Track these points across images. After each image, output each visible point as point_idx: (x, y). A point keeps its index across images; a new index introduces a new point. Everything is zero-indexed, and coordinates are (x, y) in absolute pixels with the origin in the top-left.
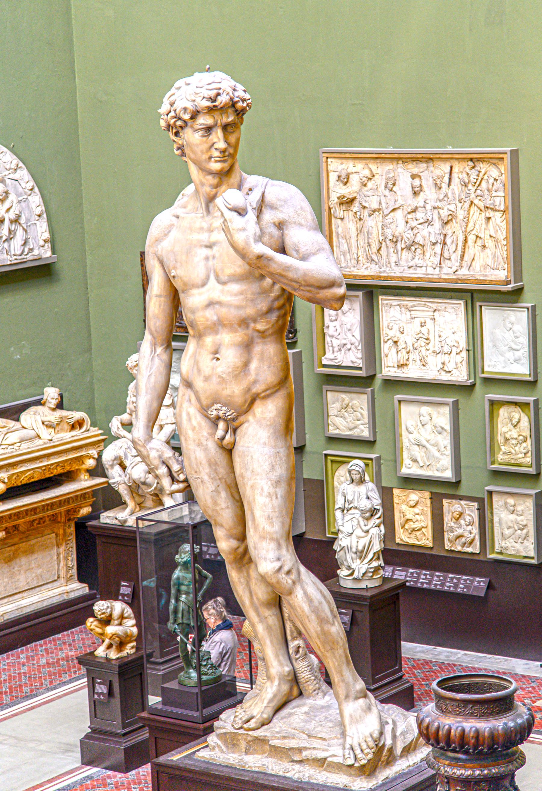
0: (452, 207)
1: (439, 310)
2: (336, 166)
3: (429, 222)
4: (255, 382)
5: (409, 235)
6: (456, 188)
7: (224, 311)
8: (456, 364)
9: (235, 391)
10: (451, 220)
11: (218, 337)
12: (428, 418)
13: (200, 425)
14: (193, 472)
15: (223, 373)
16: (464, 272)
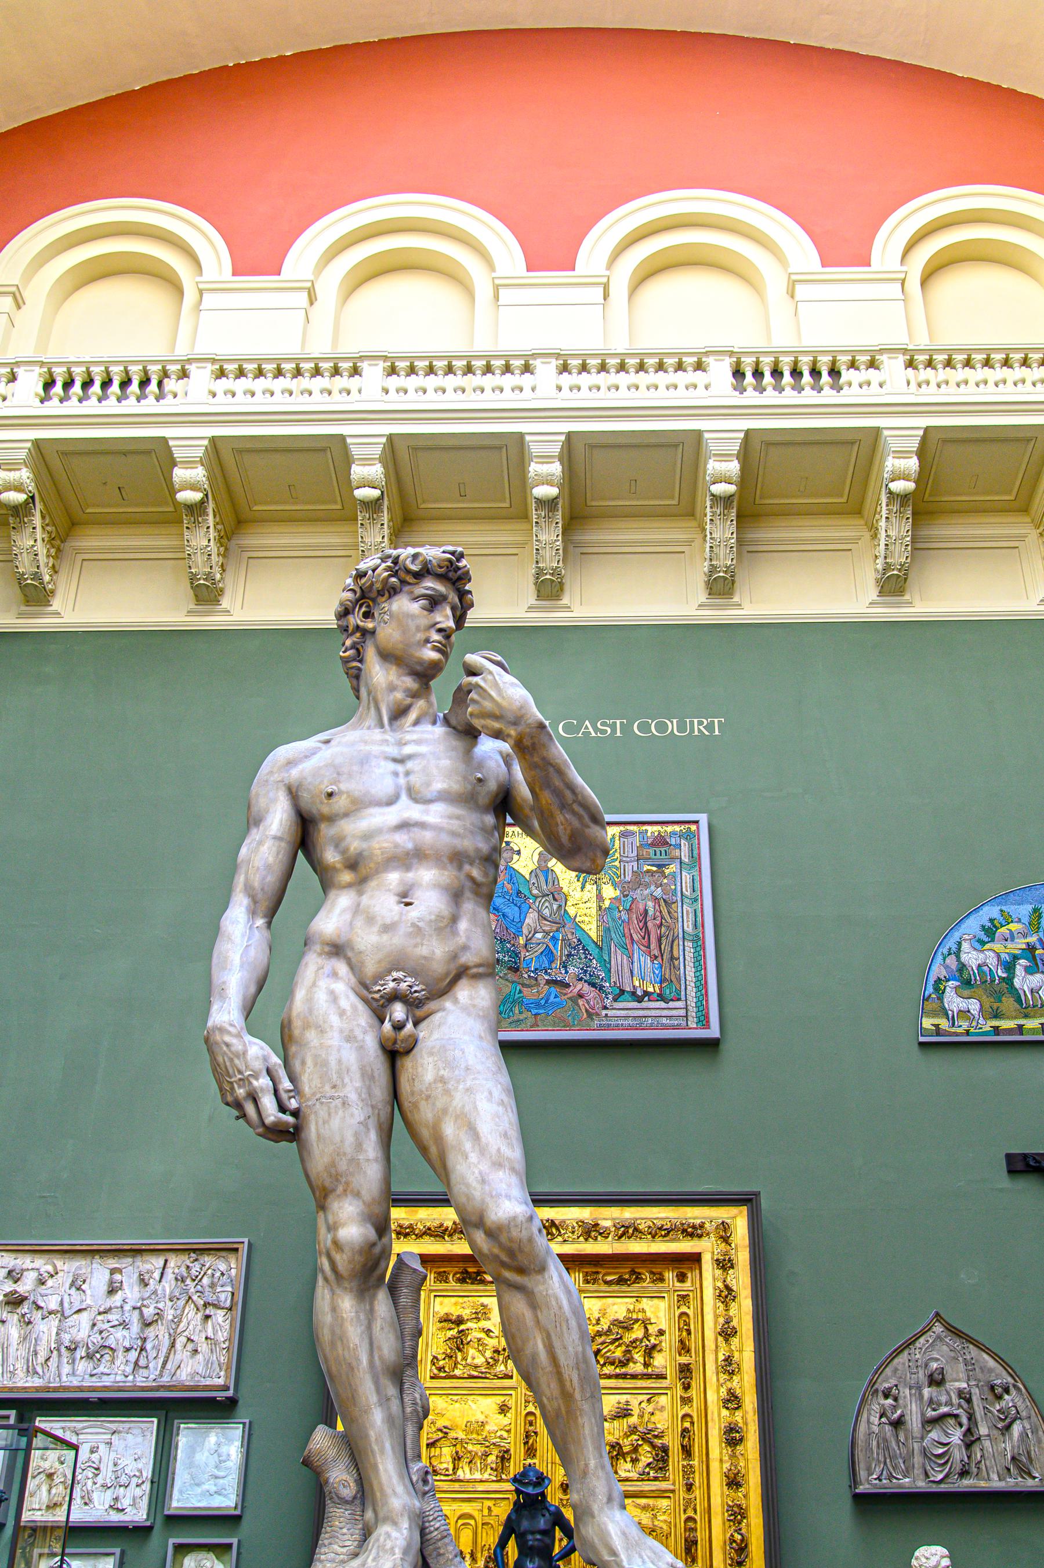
0: (161, 1305)
1: (120, 1432)
3: (124, 1325)
4: (465, 948)
5: (96, 1338)
6: (167, 1286)
7: (428, 836)
9: (435, 951)
10: (157, 1321)
11: (410, 875)
13: (354, 1008)
14: (327, 1088)
15: (420, 919)
16: (166, 1379)
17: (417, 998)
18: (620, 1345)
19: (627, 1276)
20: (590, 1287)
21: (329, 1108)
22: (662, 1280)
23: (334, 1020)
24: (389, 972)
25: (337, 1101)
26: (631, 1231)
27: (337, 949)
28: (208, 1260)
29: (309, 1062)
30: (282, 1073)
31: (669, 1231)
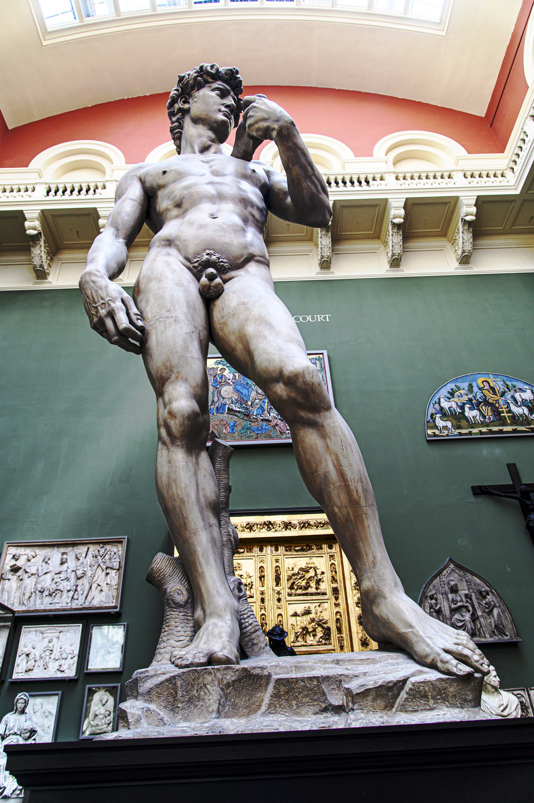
0: (85, 569)
1: (64, 632)
2: (13, 551)
3: (67, 579)
5: (54, 586)
8: (69, 665)
10: (83, 577)
12: (40, 706)
14: (164, 312)
16: (87, 605)
17: (223, 266)
18: (304, 580)
19: (305, 548)
20: (288, 553)
21: (165, 324)
22: (321, 548)
23: (169, 274)
24: (204, 250)
25: (170, 319)
26: (306, 525)
27: (169, 242)
28: (108, 547)
29: (151, 299)
30: (131, 303)
31: (324, 524)
